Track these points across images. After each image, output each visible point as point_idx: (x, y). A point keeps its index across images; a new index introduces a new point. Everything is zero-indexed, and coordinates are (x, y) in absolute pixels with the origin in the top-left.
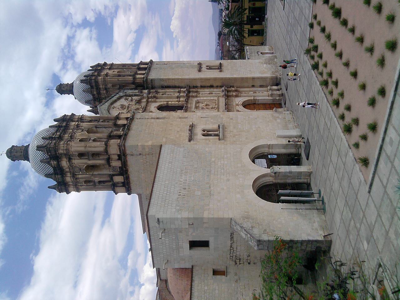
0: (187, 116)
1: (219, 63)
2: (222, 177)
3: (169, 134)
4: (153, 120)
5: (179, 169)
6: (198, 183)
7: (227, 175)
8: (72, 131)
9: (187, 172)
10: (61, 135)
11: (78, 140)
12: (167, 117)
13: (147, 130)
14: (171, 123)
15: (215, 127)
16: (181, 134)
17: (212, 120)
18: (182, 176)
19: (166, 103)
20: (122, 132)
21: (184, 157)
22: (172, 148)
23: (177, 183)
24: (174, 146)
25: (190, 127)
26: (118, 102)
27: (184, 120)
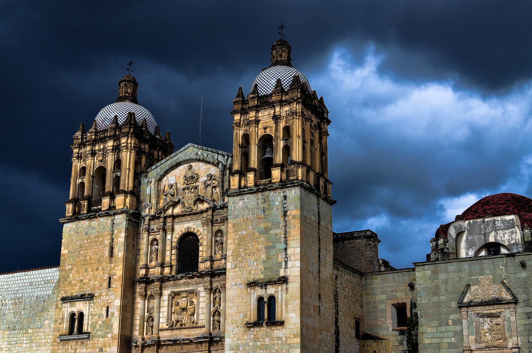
0: (114, 286)
1: (283, 319)
2: (6, 343)
3: (77, 272)
4: (107, 242)
5: (20, 295)
6: (2, 318)
7: (8, 349)
8: (100, 150)
9: (16, 304)
10: (87, 143)
11: (84, 165)
12: (114, 259)
13: (89, 240)
14: (100, 268)
15: (85, 329)
16: (76, 286)
17: (100, 322)
18: (12, 299)
19: (201, 241)
20: (85, 212)
21: (37, 297)
22: (53, 281)
23: (3, 297)
24: (56, 281)
25: (89, 294)
26: (209, 166)
27: (106, 284)
